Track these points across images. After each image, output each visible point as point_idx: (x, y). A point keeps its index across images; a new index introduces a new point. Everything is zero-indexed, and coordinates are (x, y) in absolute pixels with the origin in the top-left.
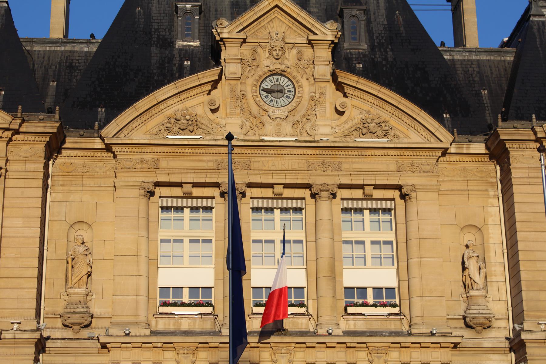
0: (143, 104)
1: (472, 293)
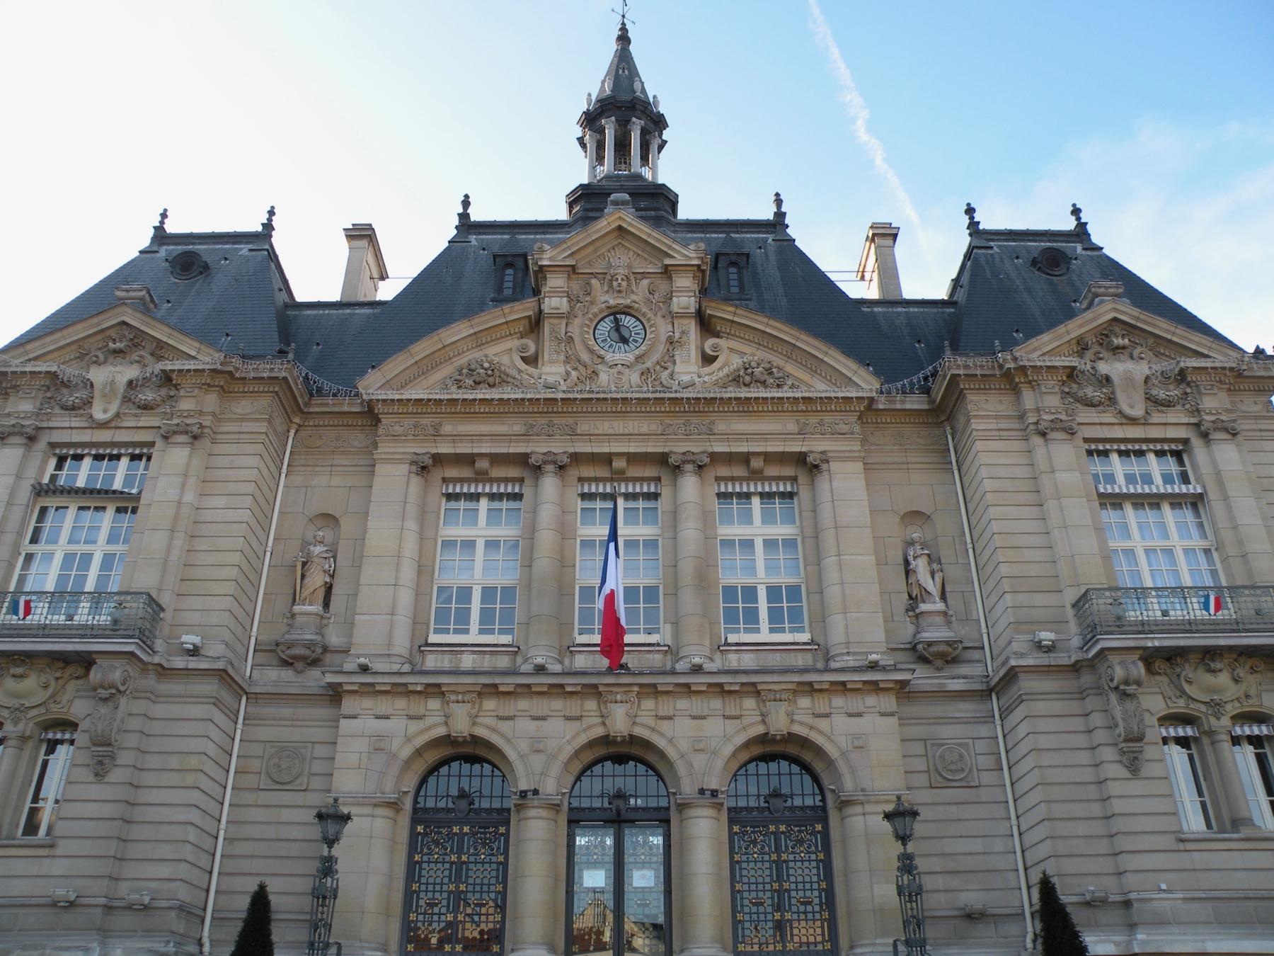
0: (422, 348)
1: (923, 607)
